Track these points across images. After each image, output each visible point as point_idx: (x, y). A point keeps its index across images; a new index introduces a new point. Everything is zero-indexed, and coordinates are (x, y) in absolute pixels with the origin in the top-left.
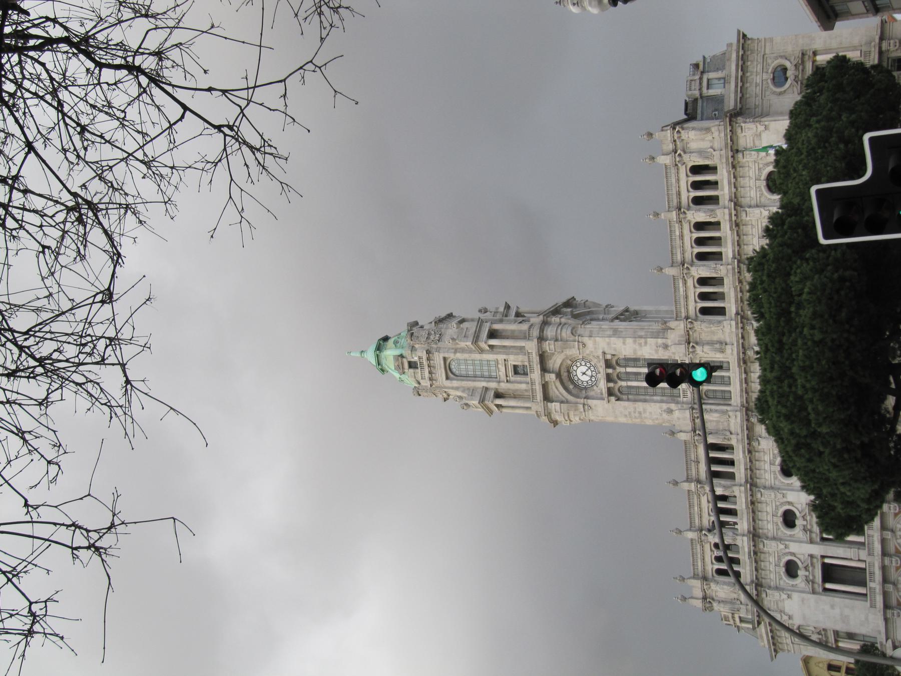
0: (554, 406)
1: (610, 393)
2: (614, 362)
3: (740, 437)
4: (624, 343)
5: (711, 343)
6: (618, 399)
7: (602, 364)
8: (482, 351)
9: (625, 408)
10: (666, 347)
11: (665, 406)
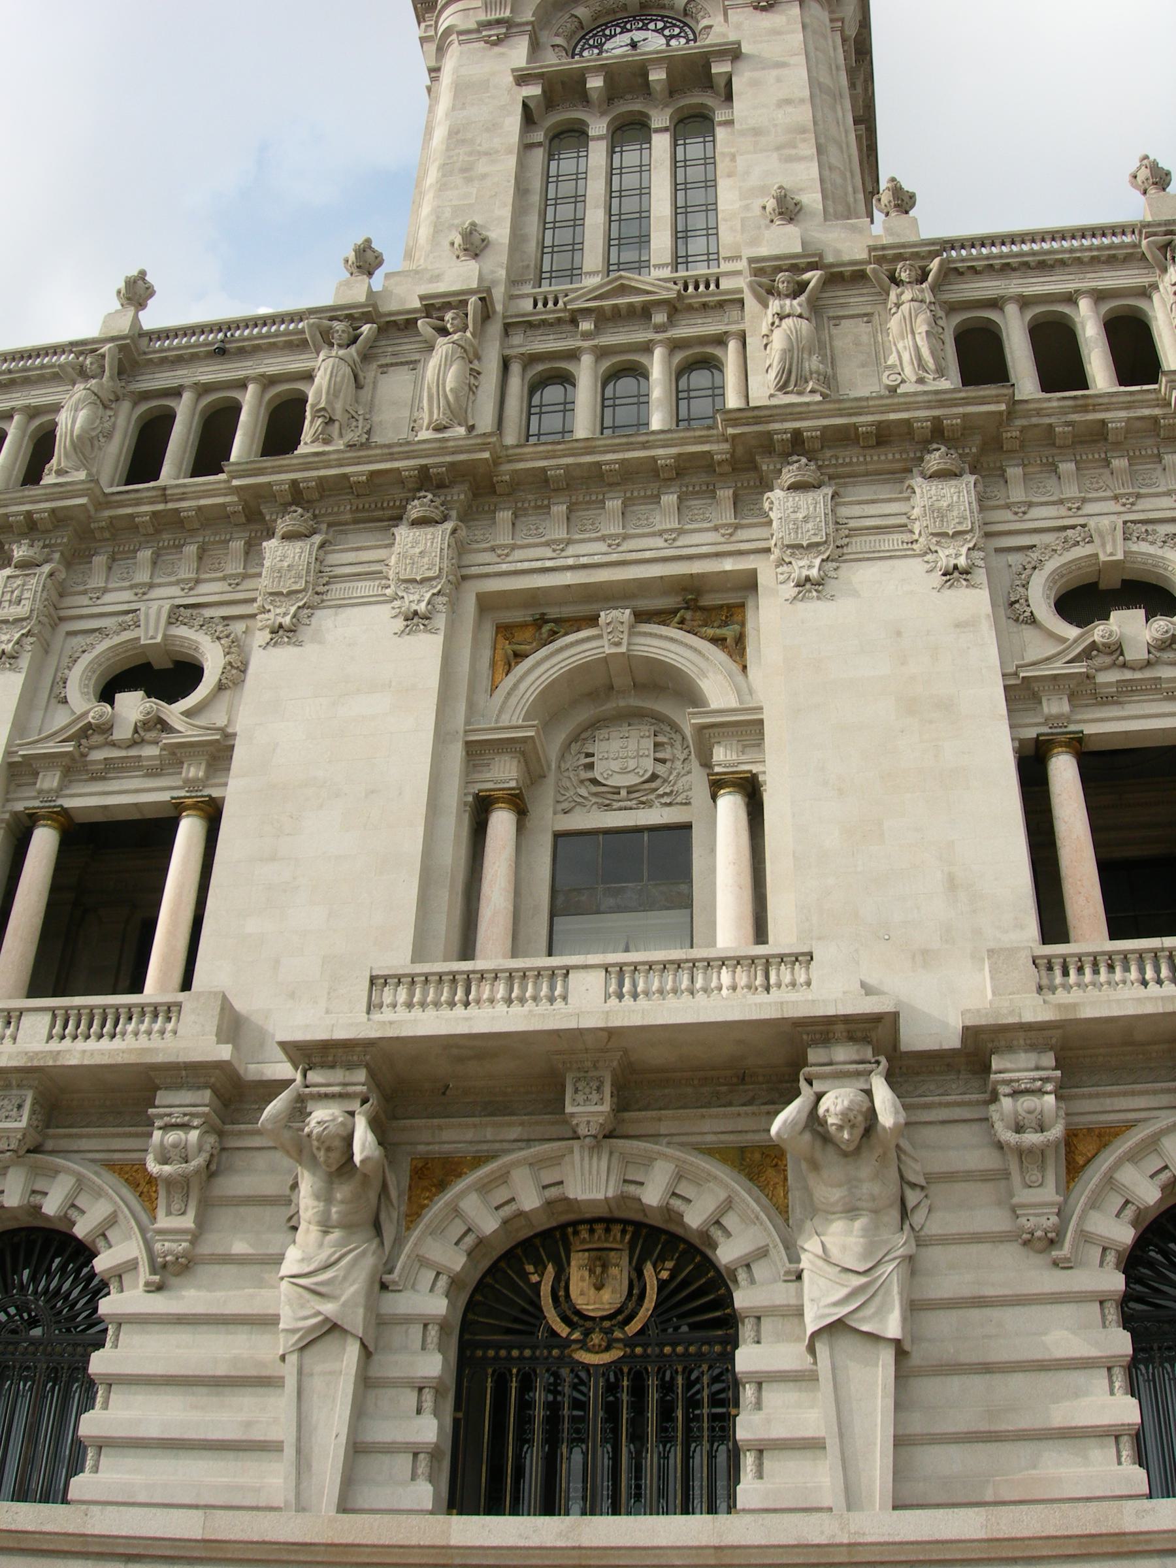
6: (529, 117)
11: (500, 234)
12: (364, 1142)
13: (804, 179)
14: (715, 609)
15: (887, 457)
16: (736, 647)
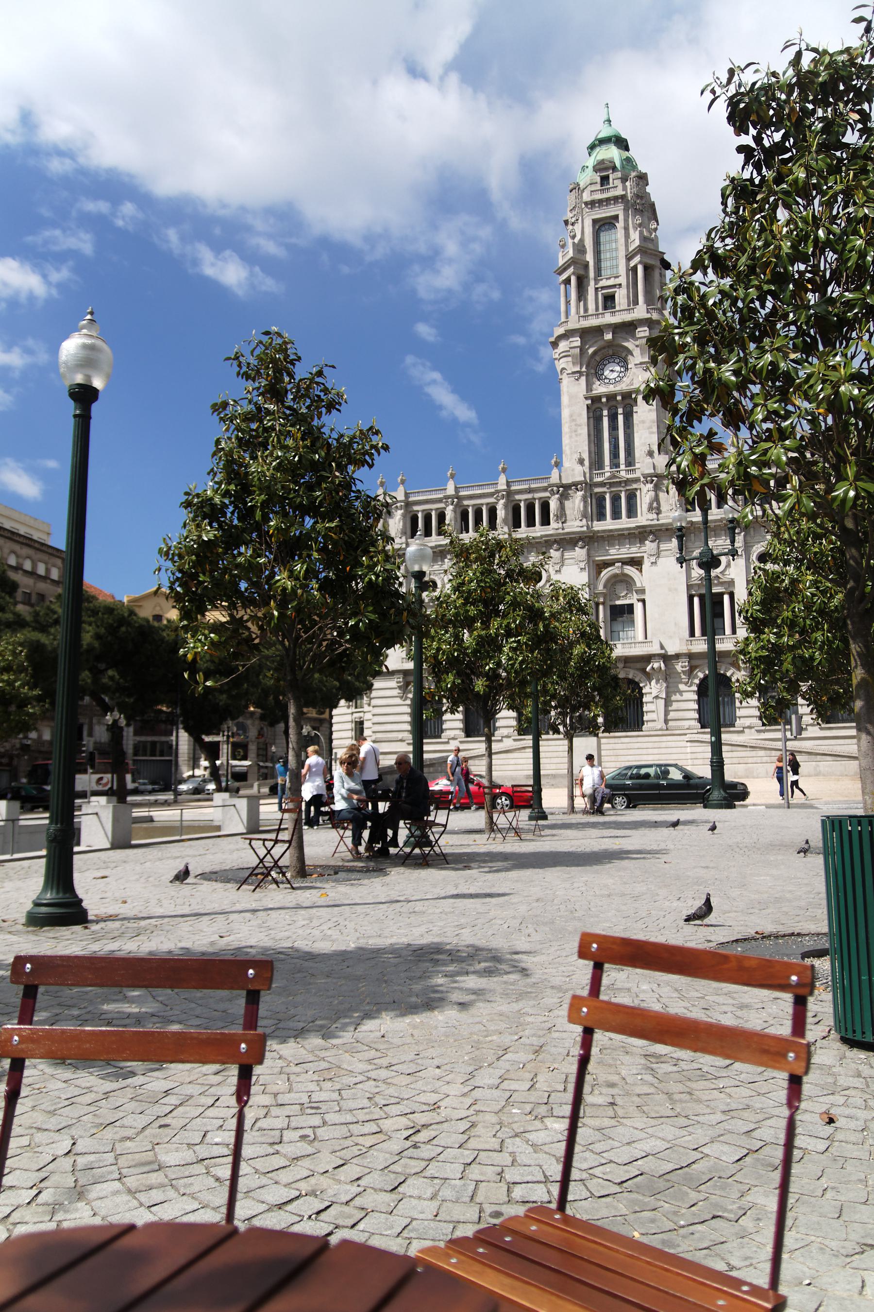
0: (576, 341)
1: (596, 400)
2: (627, 401)
3: (560, 531)
5: (657, 499)
8: (629, 259)
9: (580, 415)
10: (650, 454)
11: (586, 456)
13: (654, 440)
14: (636, 563)
15: (668, 533)
16: (641, 571)
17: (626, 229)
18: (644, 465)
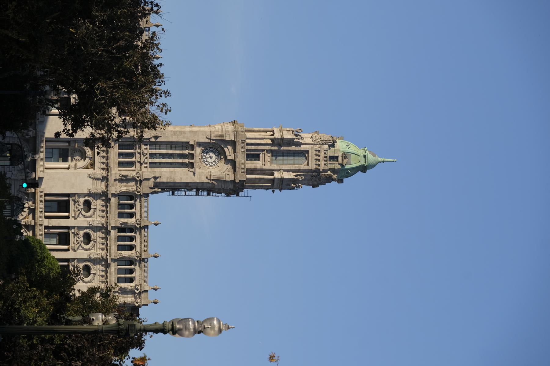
4: (181, 179)
7: (196, 165)
9: (184, 137)
11: (159, 140)
12: (27, 137)
17: (299, 171)
18: (147, 172)
